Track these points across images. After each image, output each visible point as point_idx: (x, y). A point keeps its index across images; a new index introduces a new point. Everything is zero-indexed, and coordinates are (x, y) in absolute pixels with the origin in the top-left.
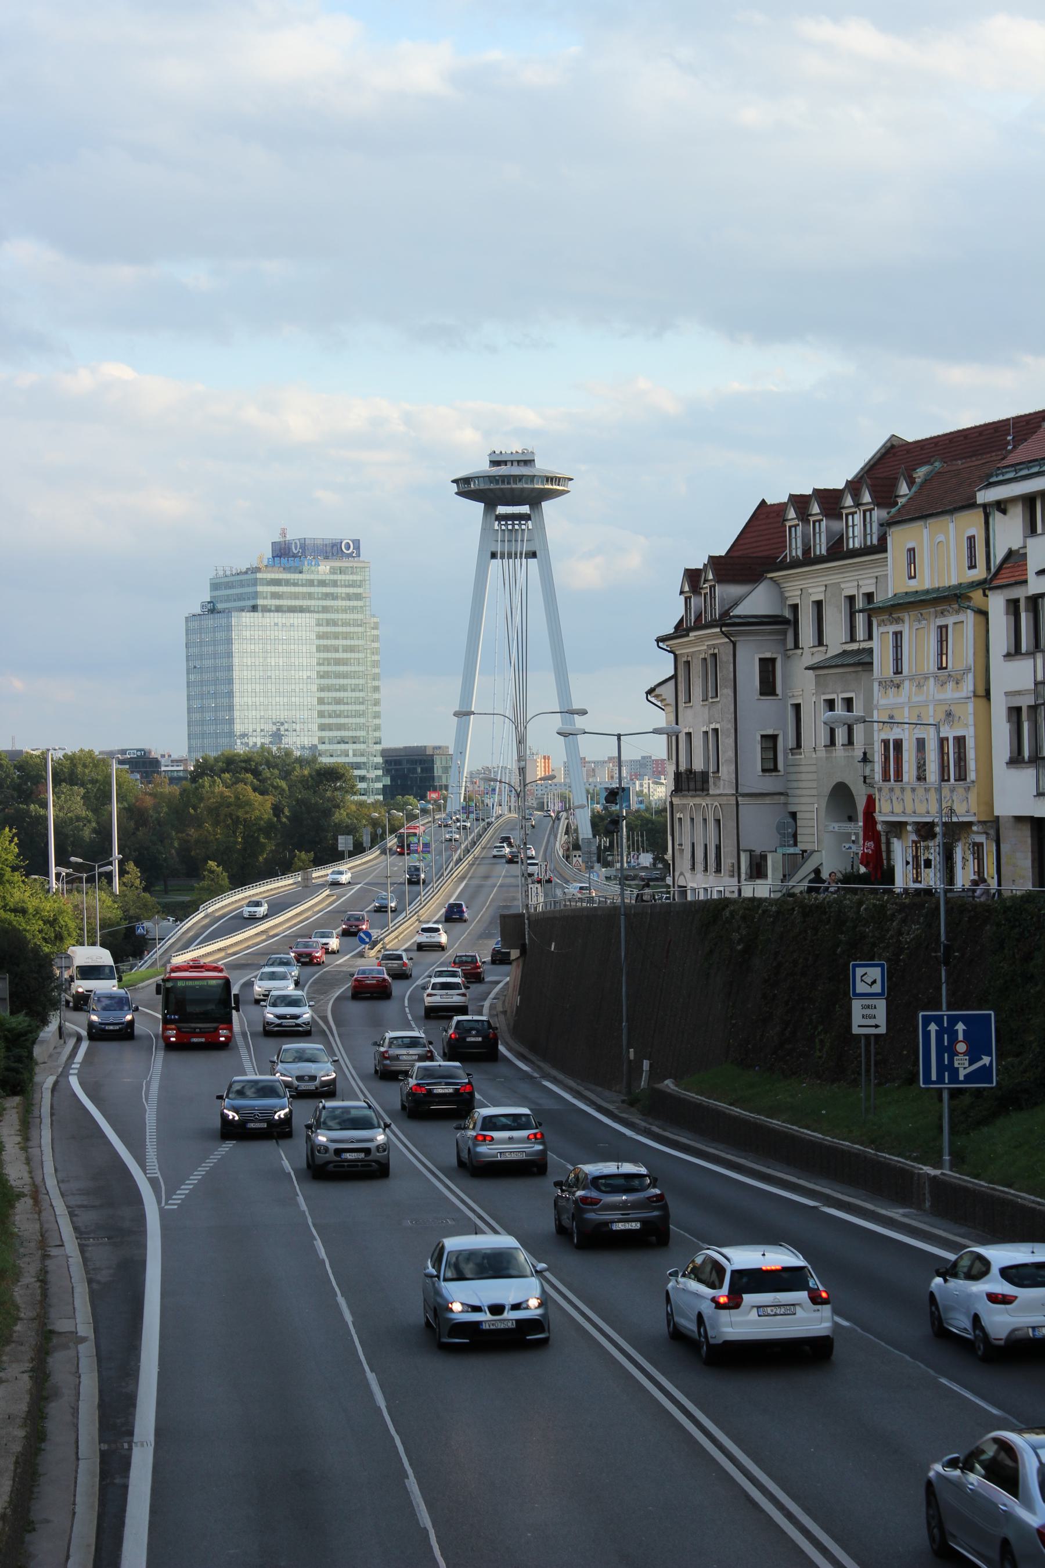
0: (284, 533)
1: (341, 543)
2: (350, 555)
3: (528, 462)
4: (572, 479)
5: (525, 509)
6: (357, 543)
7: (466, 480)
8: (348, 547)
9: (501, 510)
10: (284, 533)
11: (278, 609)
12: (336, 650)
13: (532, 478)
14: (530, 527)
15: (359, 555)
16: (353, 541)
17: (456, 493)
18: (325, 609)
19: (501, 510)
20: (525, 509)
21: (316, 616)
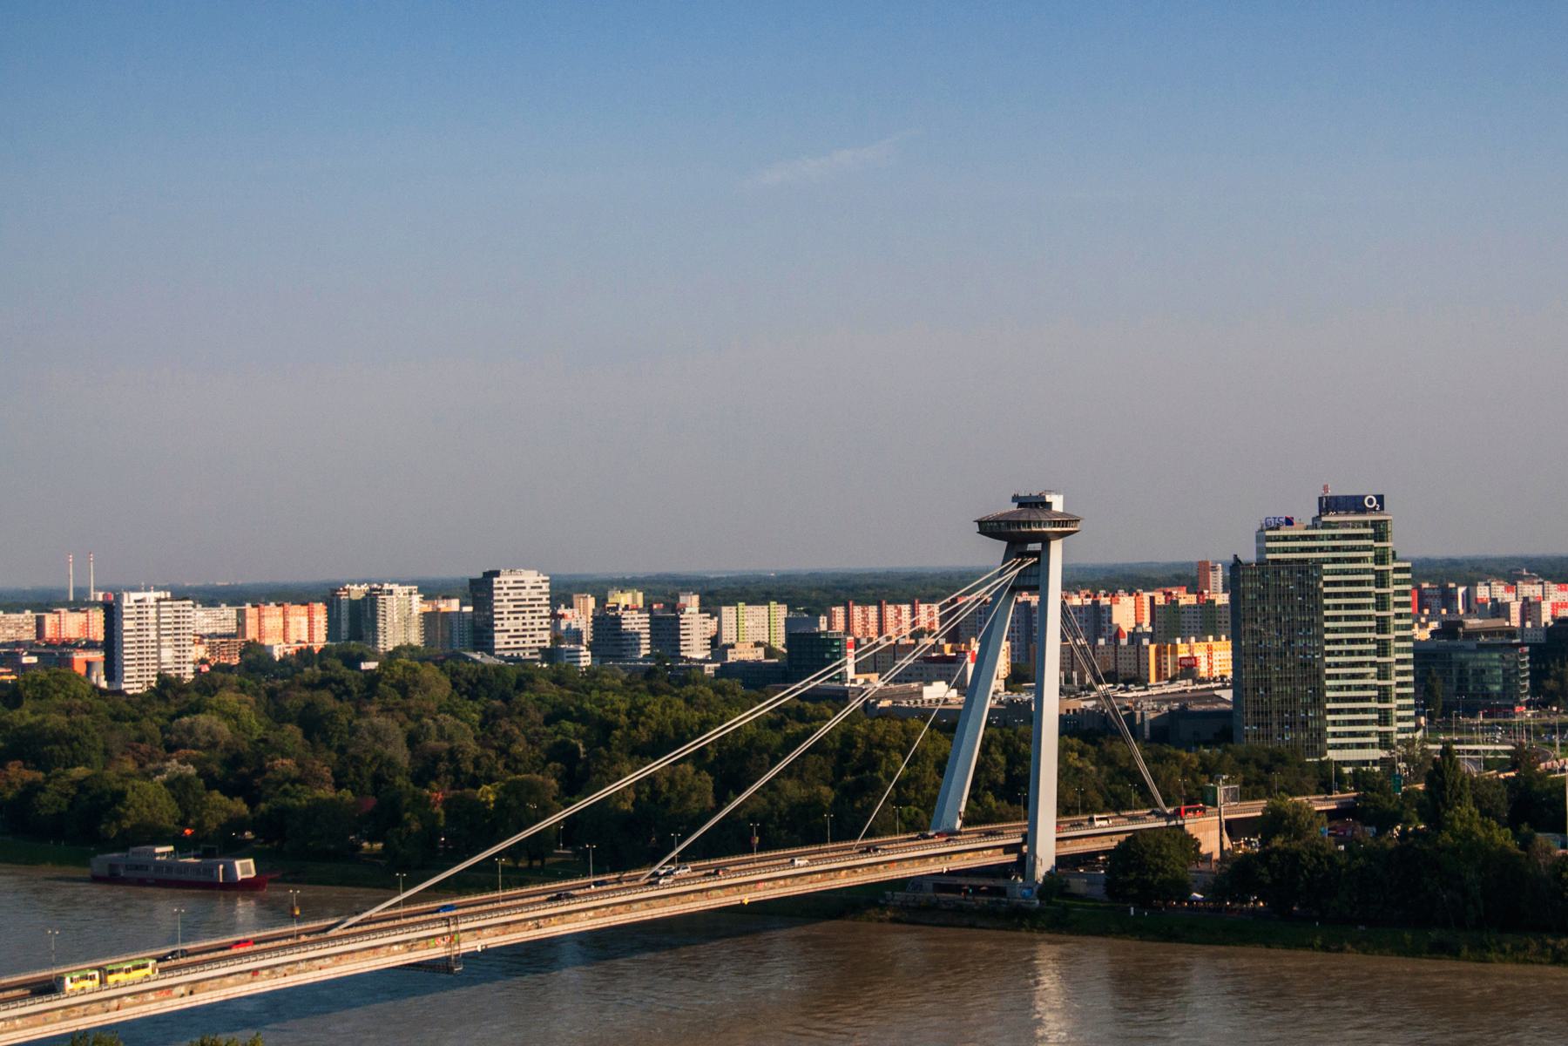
0: (1326, 488)
1: (1364, 497)
2: (1374, 509)
5: (1037, 547)
6: (1380, 499)
8: (1370, 501)
10: (1326, 488)
15: (1382, 508)
16: (1377, 497)
18: (1336, 561)
20: (1037, 547)
21: (1325, 567)
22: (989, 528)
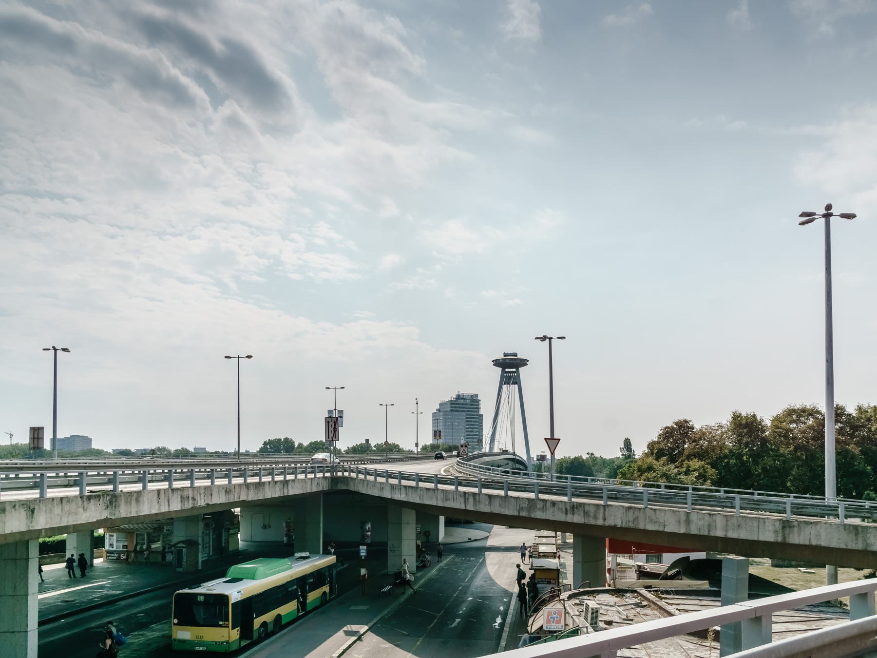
3: (516, 355)
4: (528, 361)
5: (514, 370)
6: (477, 396)
7: (496, 360)
9: (507, 370)
11: (456, 411)
12: (471, 421)
13: (516, 359)
14: (515, 374)
17: (494, 365)
18: (468, 411)
19: (507, 370)
20: (514, 370)
22: (497, 363)
